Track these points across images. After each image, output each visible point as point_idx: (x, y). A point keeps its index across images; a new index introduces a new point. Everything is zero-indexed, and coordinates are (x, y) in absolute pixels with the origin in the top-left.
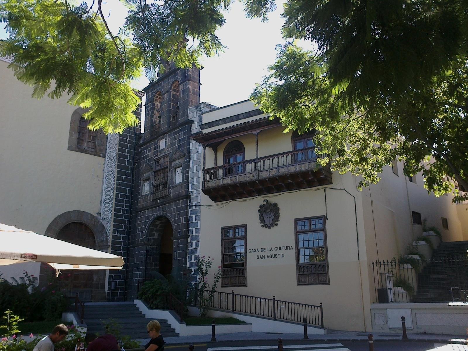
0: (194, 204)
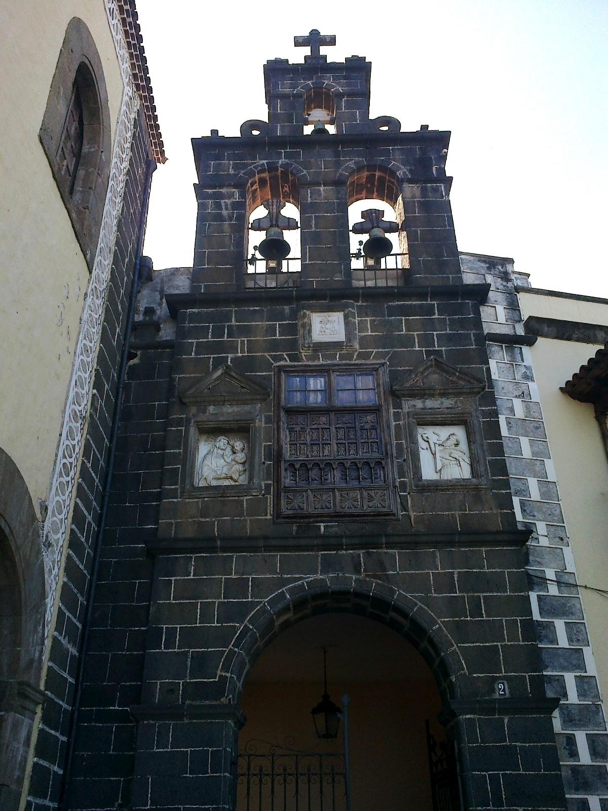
0: (550, 574)
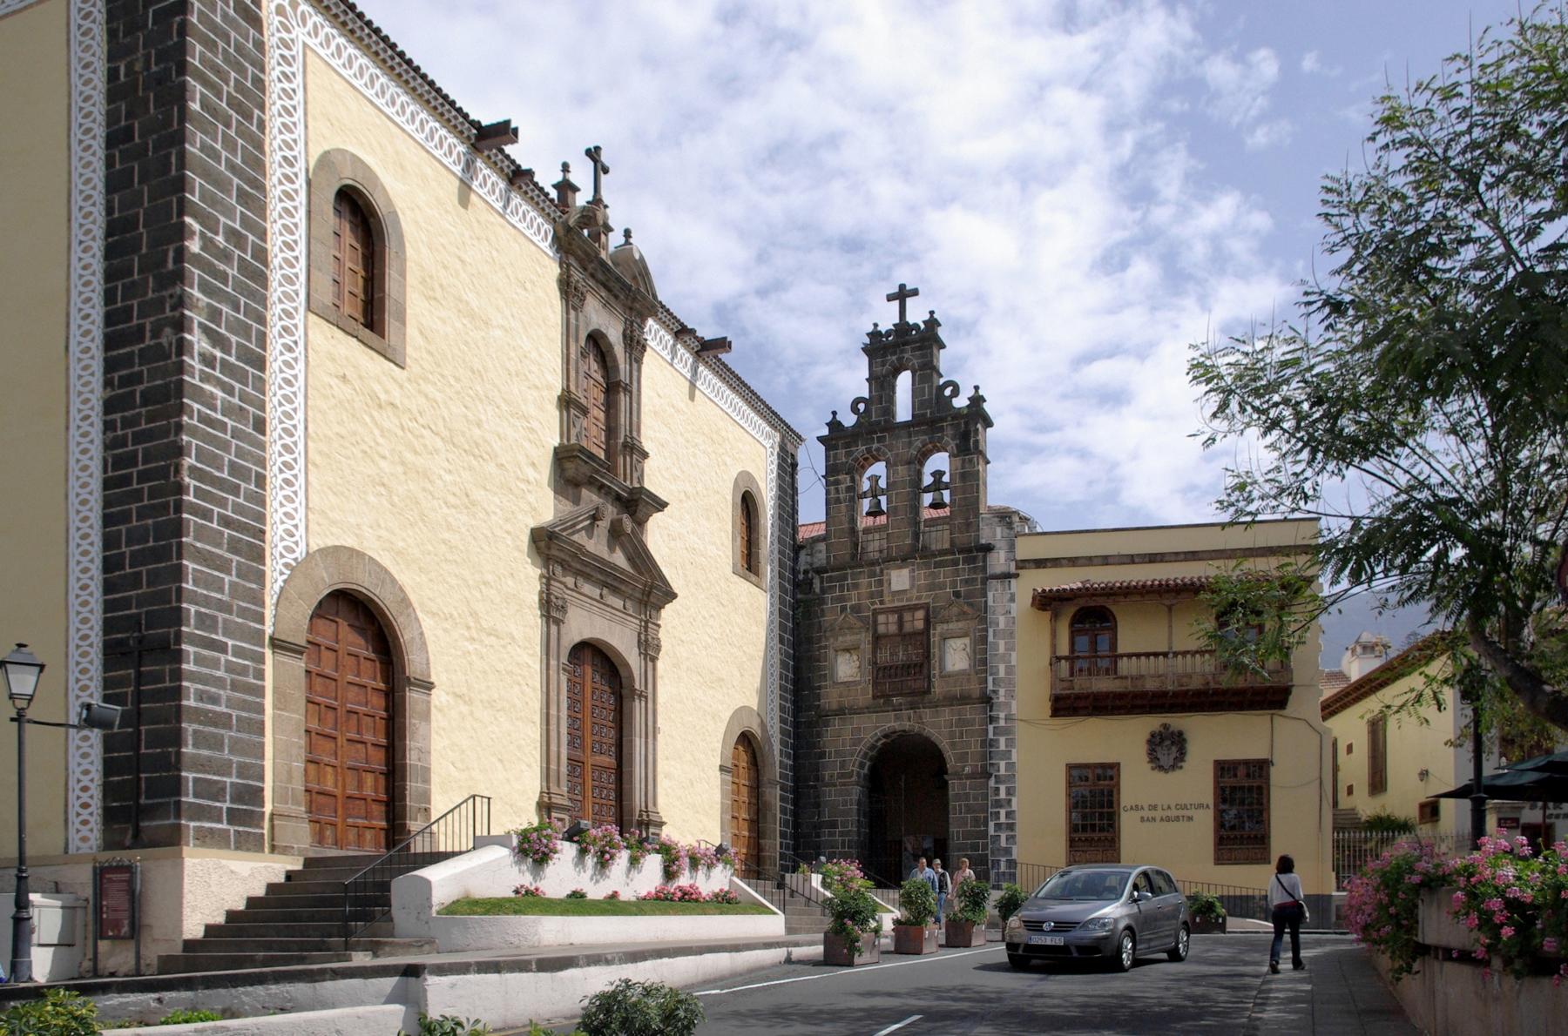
0: (1002, 715)
